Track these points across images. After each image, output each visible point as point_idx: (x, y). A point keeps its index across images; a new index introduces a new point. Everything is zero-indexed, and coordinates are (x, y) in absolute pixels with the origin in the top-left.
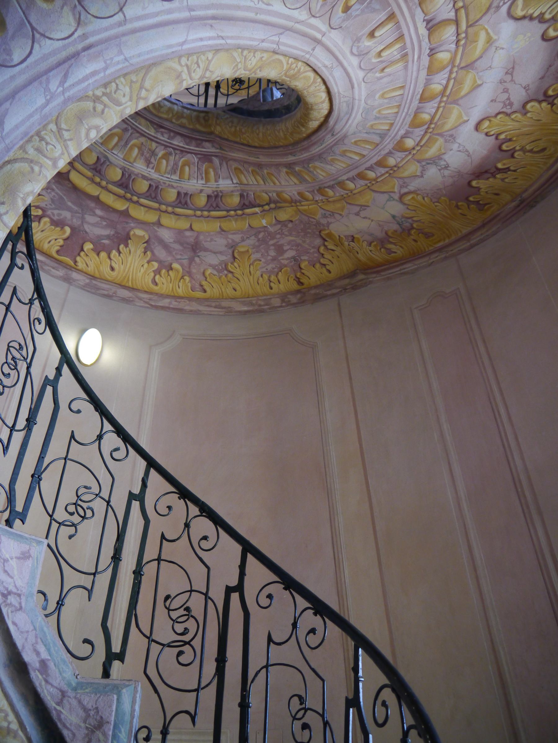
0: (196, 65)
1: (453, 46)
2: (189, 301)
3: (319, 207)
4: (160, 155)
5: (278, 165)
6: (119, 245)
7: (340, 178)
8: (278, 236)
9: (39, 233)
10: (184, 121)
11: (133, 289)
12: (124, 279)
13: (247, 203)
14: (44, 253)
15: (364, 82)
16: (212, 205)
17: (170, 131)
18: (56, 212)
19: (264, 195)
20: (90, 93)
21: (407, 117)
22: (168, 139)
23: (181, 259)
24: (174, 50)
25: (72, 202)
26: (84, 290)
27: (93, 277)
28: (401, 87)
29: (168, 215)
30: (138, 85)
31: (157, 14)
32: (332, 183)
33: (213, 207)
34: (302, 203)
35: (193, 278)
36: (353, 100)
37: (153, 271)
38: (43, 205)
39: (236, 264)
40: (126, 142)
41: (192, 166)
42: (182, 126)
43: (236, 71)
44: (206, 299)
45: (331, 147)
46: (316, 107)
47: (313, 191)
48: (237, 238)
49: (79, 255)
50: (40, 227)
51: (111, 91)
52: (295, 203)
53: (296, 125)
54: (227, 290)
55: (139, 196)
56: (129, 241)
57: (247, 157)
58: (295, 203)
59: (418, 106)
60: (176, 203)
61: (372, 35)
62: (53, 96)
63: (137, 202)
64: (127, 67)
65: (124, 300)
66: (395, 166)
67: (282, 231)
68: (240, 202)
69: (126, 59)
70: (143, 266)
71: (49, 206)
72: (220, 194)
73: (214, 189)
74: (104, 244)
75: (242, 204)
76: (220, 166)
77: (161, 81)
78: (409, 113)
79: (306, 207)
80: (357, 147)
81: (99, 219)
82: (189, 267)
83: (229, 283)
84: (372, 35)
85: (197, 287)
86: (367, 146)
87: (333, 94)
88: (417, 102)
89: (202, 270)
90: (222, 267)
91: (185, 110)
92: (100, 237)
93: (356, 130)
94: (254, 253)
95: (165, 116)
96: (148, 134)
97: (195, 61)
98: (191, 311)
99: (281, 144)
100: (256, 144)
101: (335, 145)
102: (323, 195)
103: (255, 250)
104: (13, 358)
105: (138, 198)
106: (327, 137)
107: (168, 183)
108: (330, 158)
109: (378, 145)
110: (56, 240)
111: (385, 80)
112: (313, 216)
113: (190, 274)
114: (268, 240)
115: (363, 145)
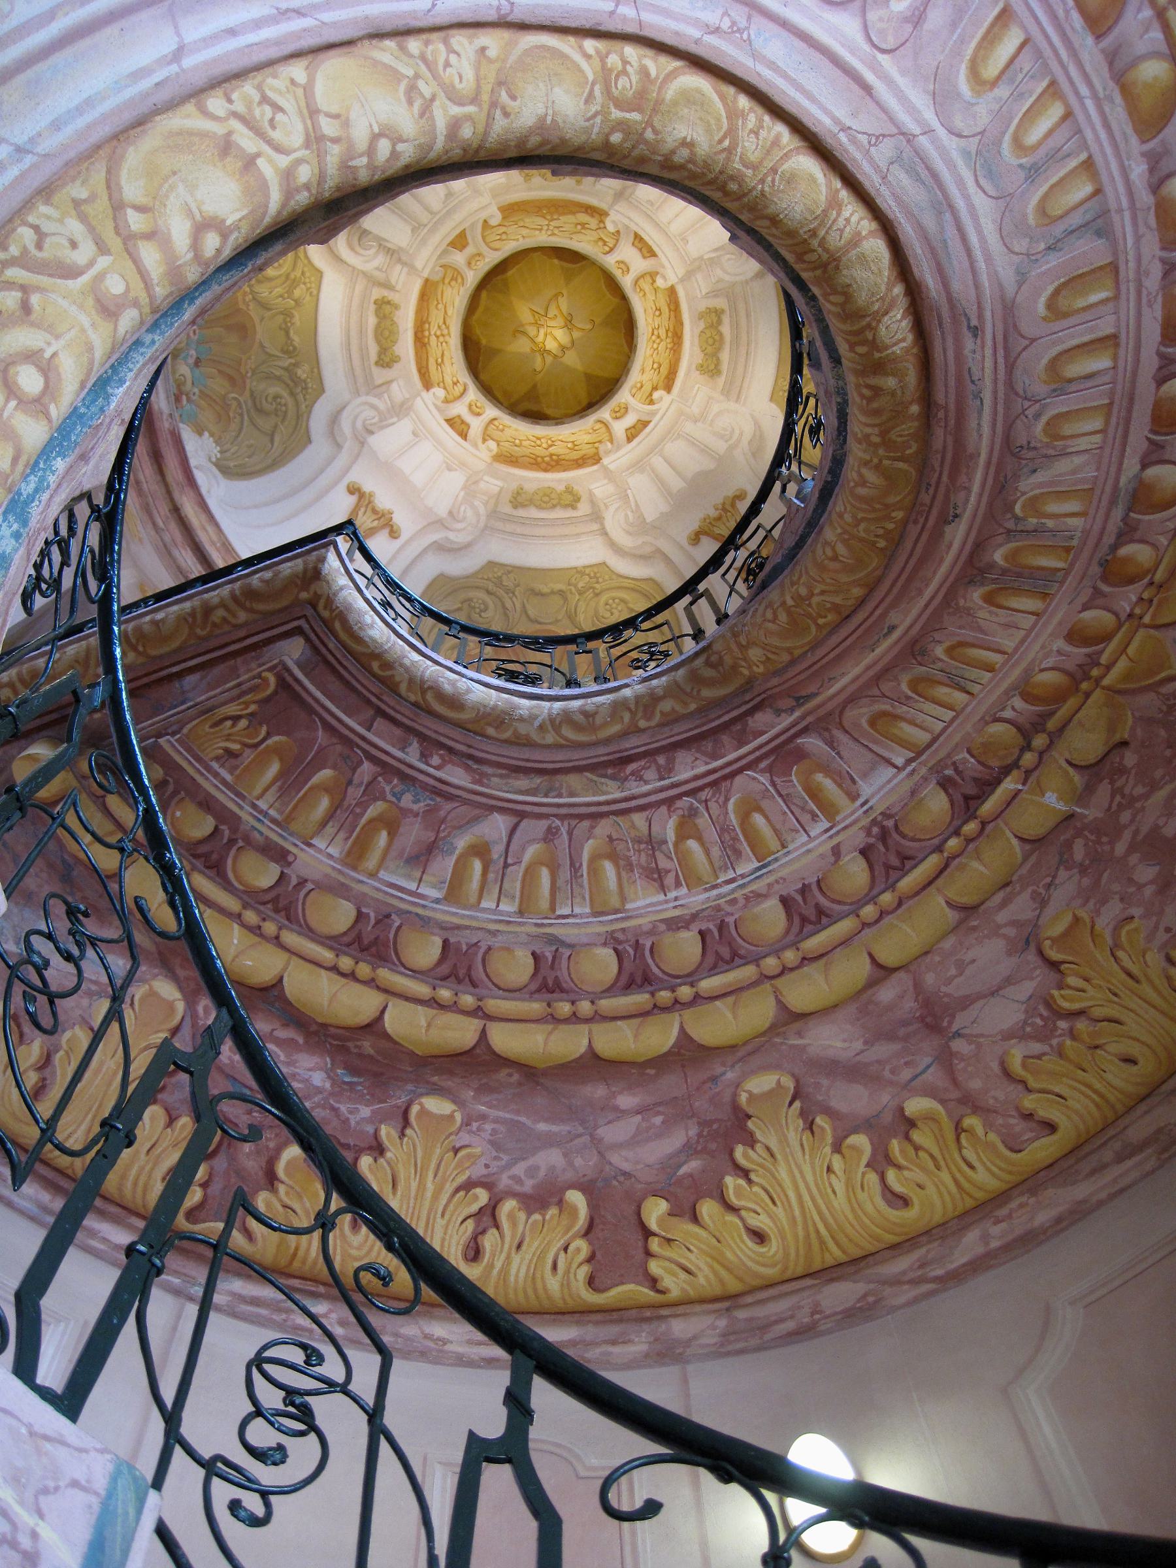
0: (268, 110)
2: (1033, 1192)
3: (1152, 631)
4: (671, 836)
5: (949, 599)
6: (731, 1152)
7: (1123, 480)
8: (1125, 817)
9: (516, 1259)
10: (667, 705)
11: (854, 1261)
12: (809, 1246)
13: (971, 790)
14: (563, 1313)
15: (883, 51)
16: (888, 867)
17: (650, 754)
18: (519, 1169)
19: (997, 728)
21: (1107, 109)
22: (662, 778)
23: (916, 1076)
24: (158, 77)
25: (546, 1120)
26: (728, 1354)
27: (728, 1300)
28: (999, 17)
29: (793, 975)
30: (103, 203)
32: (1118, 513)
33: (895, 868)
34: (1104, 660)
35: (988, 1110)
36: (908, 141)
37: (868, 1165)
38: (478, 1171)
39: (1072, 980)
40: (572, 864)
41: (765, 804)
42: (671, 720)
43: (426, 111)
44: (1077, 1151)
45: (1010, 384)
46: (835, 241)
47: (1097, 592)
48: (1021, 907)
49: (649, 1254)
50: (508, 1239)
51: (25, 247)
52: (1087, 677)
53: (865, 391)
54: (1109, 1076)
55: (691, 978)
56: (750, 1124)
57: (870, 658)
58: (1087, 677)
59: (1103, 51)
60: (795, 929)
63: (697, 999)
64: (34, 166)
65: (853, 1315)
67: (1123, 796)
68: (952, 805)
69: (19, 150)
70: (829, 1169)
71: (495, 1166)
72: (890, 823)
73: (865, 822)
74: (691, 1175)
75: (961, 800)
76: (833, 749)
77: (174, 173)
78: (1101, 95)
79: (1122, 664)
80: (1065, 323)
81: (639, 1117)
82: (955, 1081)
83: (1099, 1051)
85: (1017, 1129)
86: (1094, 298)
87: (829, 141)
88: (1090, 40)
89: (995, 1066)
90: (1041, 1016)
91: (655, 682)
92: (669, 1165)
93: (1016, 259)
94: (1098, 912)
95: (616, 728)
96: (608, 803)
97: (256, 97)
98: (1059, 1220)
99: (899, 515)
100: (857, 592)
101: (1010, 367)
102: (1131, 581)
103: (1092, 902)
104: (291, 1393)
105: (692, 985)
106: (966, 352)
107: (738, 894)
109: (1113, 268)
110: (566, 1249)
112: (1163, 675)
113: (971, 1103)
114: (1107, 848)
115: (1080, 303)
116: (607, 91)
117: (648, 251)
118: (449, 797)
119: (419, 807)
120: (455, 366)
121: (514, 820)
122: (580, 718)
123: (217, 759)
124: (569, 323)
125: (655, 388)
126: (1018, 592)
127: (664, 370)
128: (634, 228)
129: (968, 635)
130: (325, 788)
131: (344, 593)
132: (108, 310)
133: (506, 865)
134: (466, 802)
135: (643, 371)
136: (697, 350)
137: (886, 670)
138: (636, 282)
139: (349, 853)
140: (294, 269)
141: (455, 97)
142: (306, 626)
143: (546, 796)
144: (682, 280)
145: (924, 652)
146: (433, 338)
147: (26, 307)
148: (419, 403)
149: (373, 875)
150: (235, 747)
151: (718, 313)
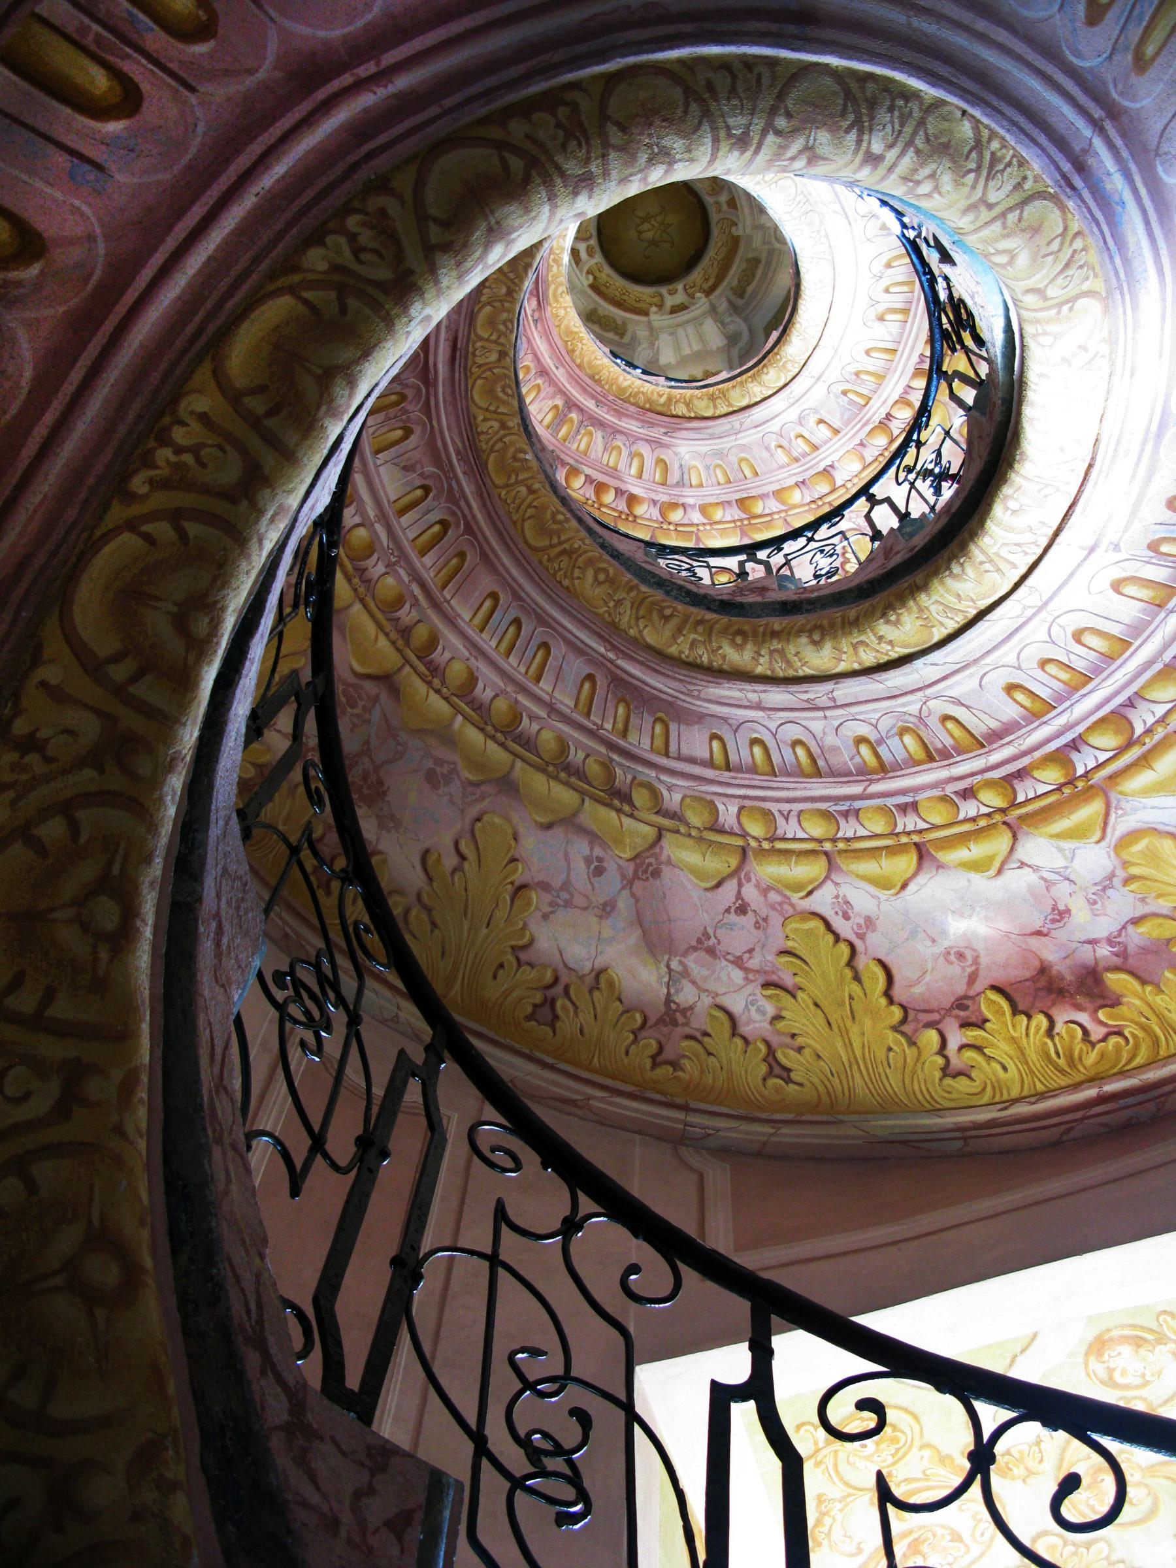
1: (808, 499)
5: (562, 392)
10: (555, 269)
32: (572, 462)
57: (546, 356)
61: (821, 421)
66: (635, 517)
84: (821, 421)
100: (578, 361)
108: (620, 444)
111: (765, 454)
117: (676, 309)
124: (654, 243)
125: (595, 278)
126: (555, 418)
127: (603, 289)
128: (693, 308)
129: (542, 395)
135: (608, 276)
136: (606, 313)
137: (538, 360)
138: (661, 295)
144: (649, 322)
145: (541, 375)
151: (622, 335)
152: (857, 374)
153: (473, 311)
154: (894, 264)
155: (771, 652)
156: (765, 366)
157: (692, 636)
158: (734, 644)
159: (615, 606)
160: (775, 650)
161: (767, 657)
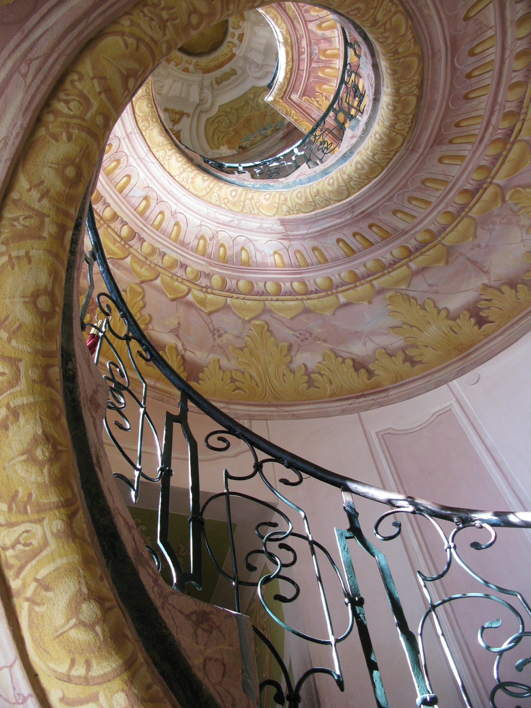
20: (226, 208)
31: (189, 213)
43: (170, 156)
62: (239, 220)
116: (149, 127)
118: (310, 42)
119: (316, 47)
120: (224, 49)
121: (308, 22)
122: (275, 20)
123: (329, 101)
130: (323, 72)
131: (276, 92)
132: (221, 188)
133: (320, 18)
134: (309, 37)
139: (336, 58)
140: (222, 115)
141: (166, 152)
142: (288, 97)
143: (298, 18)
146: (219, 61)
147: (226, 198)
148: (241, 55)
149: (339, 49)
150: (324, 98)
152: (118, 161)
153: (412, 19)
154: (176, 228)
155: (42, 216)
156: (152, 107)
157: (95, 105)
158: (68, 161)
159: (161, 18)
160: (42, 223)
161: (37, 206)
